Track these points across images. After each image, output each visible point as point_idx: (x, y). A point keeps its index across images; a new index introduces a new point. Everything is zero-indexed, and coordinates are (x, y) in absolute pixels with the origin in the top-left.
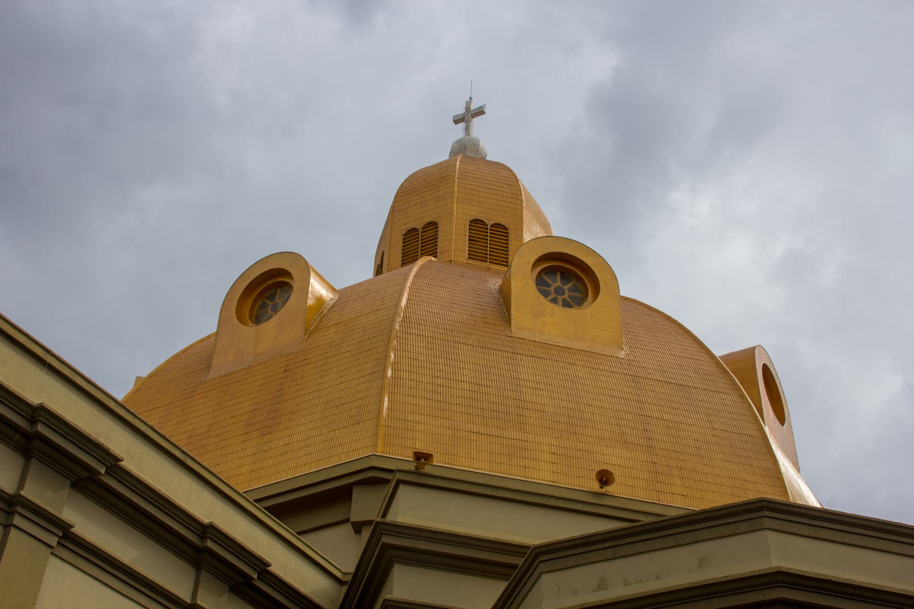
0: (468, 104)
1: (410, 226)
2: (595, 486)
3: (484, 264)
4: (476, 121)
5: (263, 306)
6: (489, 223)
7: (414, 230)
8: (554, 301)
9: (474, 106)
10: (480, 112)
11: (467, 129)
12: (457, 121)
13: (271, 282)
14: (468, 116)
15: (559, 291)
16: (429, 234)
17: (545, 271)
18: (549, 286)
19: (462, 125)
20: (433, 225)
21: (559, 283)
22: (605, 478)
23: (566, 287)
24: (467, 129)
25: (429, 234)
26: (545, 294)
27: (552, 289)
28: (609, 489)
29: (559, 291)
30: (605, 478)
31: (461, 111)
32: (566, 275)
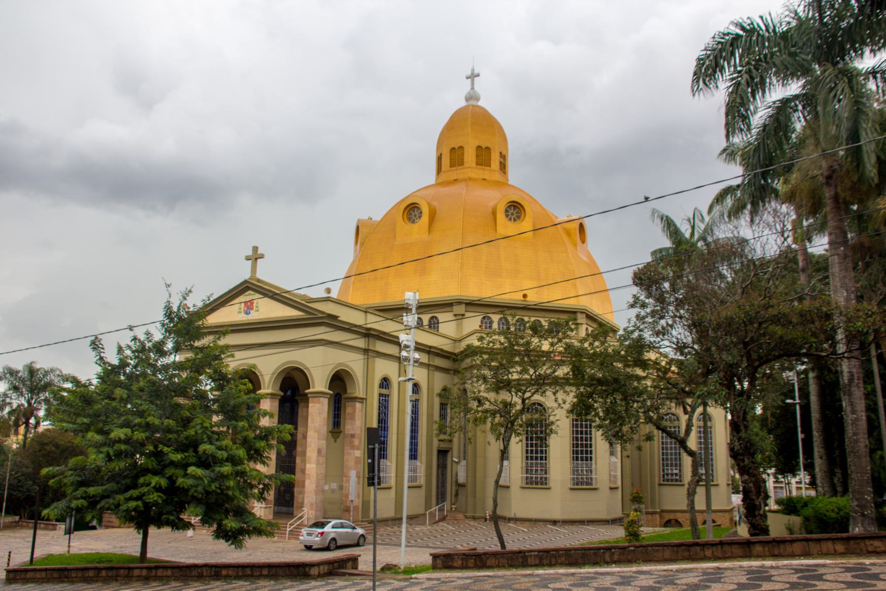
0: (473, 70)
1: (453, 146)
2: (522, 298)
3: (482, 167)
4: (476, 79)
5: (411, 214)
6: (484, 147)
7: (453, 149)
8: (510, 219)
9: (476, 72)
11: (473, 84)
12: (467, 78)
14: (473, 76)
15: (512, 214)
17: (509, 207)
19: (469, 80)
20: (461, 148)
24: (473, 84)
26: (507, 216)
29: (512, 214)
30: (525, 296)
31: (469, 73)
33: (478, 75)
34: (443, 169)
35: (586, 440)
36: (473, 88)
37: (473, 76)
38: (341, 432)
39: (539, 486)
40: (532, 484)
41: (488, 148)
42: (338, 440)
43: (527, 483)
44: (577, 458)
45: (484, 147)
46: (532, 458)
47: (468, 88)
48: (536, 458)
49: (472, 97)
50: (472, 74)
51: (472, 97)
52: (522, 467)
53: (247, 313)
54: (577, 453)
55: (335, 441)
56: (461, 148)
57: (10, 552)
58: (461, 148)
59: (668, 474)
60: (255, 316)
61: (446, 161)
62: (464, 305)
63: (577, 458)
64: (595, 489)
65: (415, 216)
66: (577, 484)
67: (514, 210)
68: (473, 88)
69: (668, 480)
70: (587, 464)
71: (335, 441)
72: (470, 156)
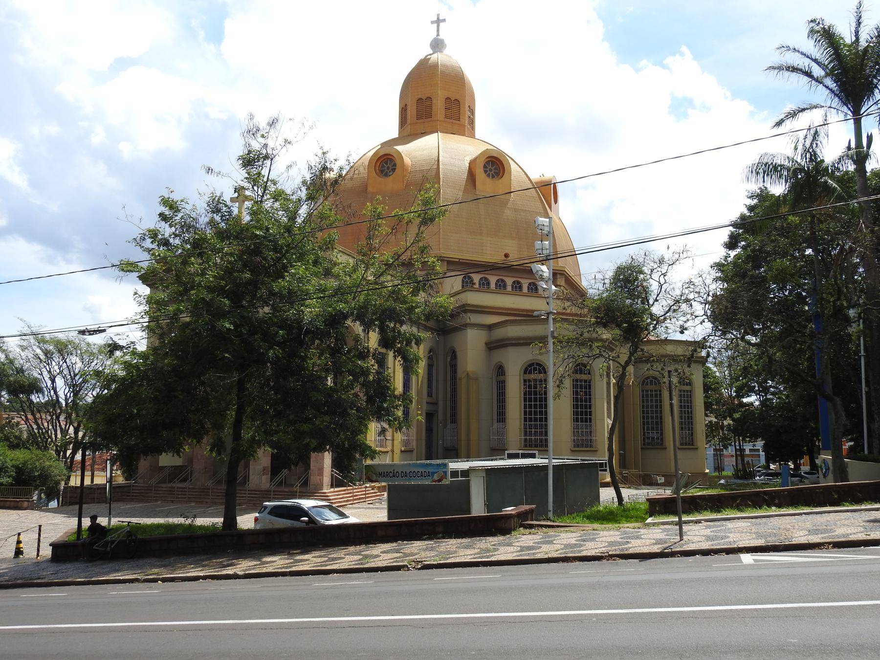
1: (420, 97)
2: (504, 258)
6: (453, 99)
7: (421, 99)
8: (488, 176)
9: (441, 18)
10: (444, 20)
11: (438, 30)
12: (432, 22)
13: (385, 157)
14: (438, 21)
15: (491, 170)
16: (428, 103)
18: (487, 168)
21: (490, 167)
22: (506, 256)
23: (493, 168)
24: (438, 30)
25: (428, 103)
26: (486, 172)
27: (488, 169)
28: (509, 258)
29: (491, 170)
30: (506, 256)
32: (493, 163)
34: (409, 121)
35: (586, 401)
36: (438, 35)
37: (438, 21)
41: (456, 100)
44: (577, 418)
45: (453, 99)
47: (435, 35)
49: (437, 45)
50: (438, 18)
51: (437, 45)
52: (520, 429)
54: (577, 415)
56: (429, 99)
57: (40, 526)
58: (429, 99)
59: (648, 438)
62: (446, 263)
63: (577, 418)
64: (596, 451)
65: (388, 168)
66: (578, 446)
67: (492, 166)
68: (438, 35)
69: (648, 444)
70: (587, 426)
72: (439, 107)
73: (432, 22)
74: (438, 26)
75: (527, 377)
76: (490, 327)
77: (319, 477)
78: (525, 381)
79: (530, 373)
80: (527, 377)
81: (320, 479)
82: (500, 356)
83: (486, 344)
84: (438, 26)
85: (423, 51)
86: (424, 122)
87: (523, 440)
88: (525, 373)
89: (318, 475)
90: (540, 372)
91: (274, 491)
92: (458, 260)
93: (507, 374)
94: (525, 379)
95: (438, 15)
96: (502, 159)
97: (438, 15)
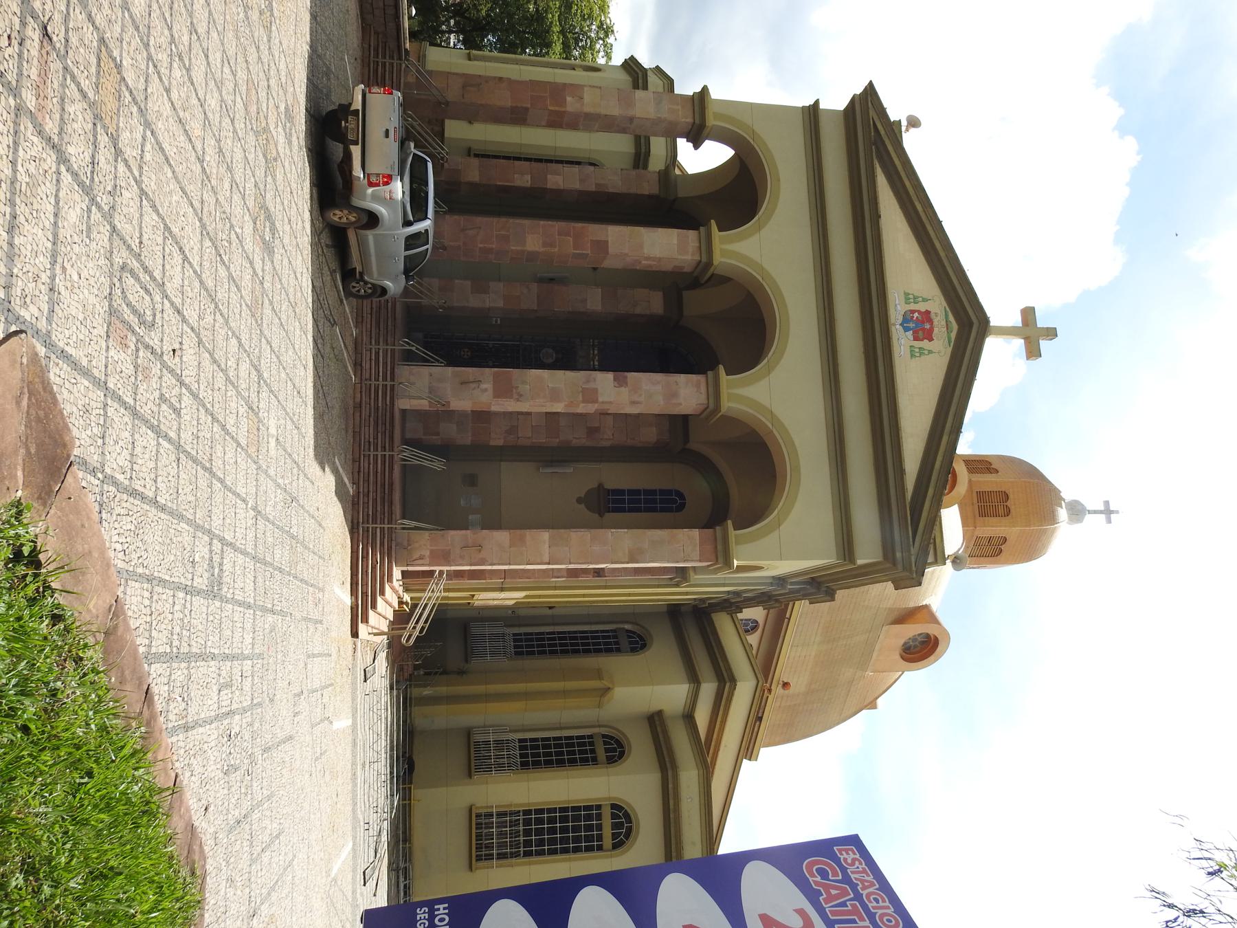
1: (1011, 496)
6: (1002, 547)
11: (1095, 512)
12: (1107, 503)
14: (1108, 512)
16: (1001, 511)
24: (1095, 512)
25: (1001, 511)
30: (786, 685)
33: (1109, 521)
36: (1090, 512)
37: (1108, 512)
38: (601, 515)
39: (474, 830)
40: (479, 826)
41: (1001, 551)
42: (582, 506)
43: (478, 816)
45: (1002, 547)
46: (527, 822)
48: (527, 833)
49: (1077, 511)
50: (1112, 512)
51: (1077, 511)
52: (511, 805)
53: (907, 318)
55: (579, 501)
56: (1008, 513)
58: (1008, 513)
60: (902, 341)
61: (987, 482)
68: (1090, 512)
71: (579, 501)
72: (993, 528)
73: (1107, 503)
74: (1101, 512)
75: (607, 813)
76: (689, 717)
77: (428, 553)
78: (599, 807)
79: (614, 816)
80: (607, 813)
81: (421, 558)
82: (640, 746)
83: (660, 713)
84: (1101, 512)
85: (1067, 494)
86: (973, 504)
87: (489, 810)
88: (614, 806)
89: (432, 552)
90: (614, 836)
91: (392, 457)
92: (788, 616)
93: (613, 769)
94: (603, 808)
95: (1117, 512)
96: (932, 658)
97: (1117, 512)
